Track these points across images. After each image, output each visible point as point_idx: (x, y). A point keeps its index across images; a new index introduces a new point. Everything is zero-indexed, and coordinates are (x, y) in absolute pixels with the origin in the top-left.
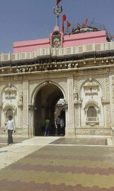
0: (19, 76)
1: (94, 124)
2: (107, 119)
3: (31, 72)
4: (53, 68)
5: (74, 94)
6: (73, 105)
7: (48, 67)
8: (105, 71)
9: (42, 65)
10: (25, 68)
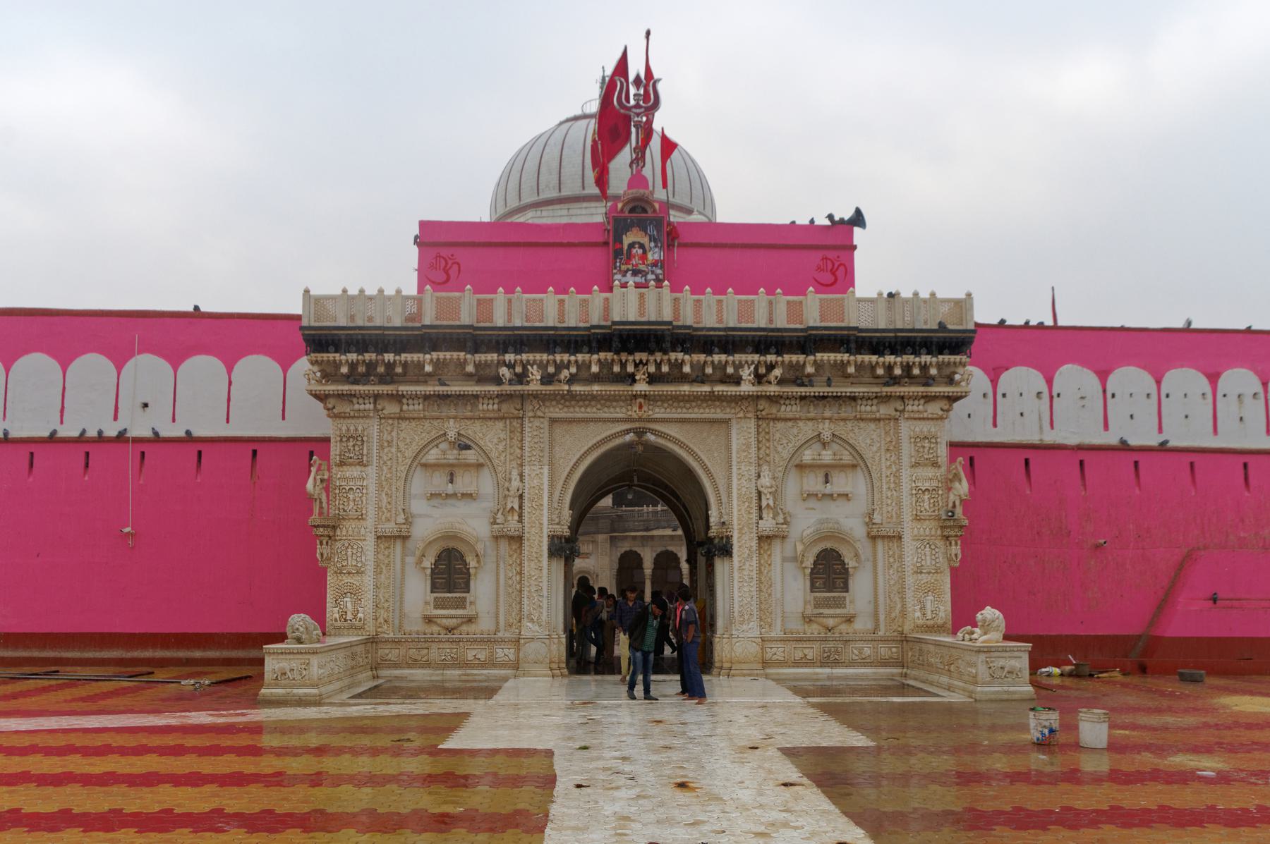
0: (504, 398)
1: (836, 620)
2: (888, 601)
3: (573, 388)
5: (759, 494)
6: (754, 543)
7: (652, 369)
8: (884, 410)
9: (624, 359)
10: (542, 366)
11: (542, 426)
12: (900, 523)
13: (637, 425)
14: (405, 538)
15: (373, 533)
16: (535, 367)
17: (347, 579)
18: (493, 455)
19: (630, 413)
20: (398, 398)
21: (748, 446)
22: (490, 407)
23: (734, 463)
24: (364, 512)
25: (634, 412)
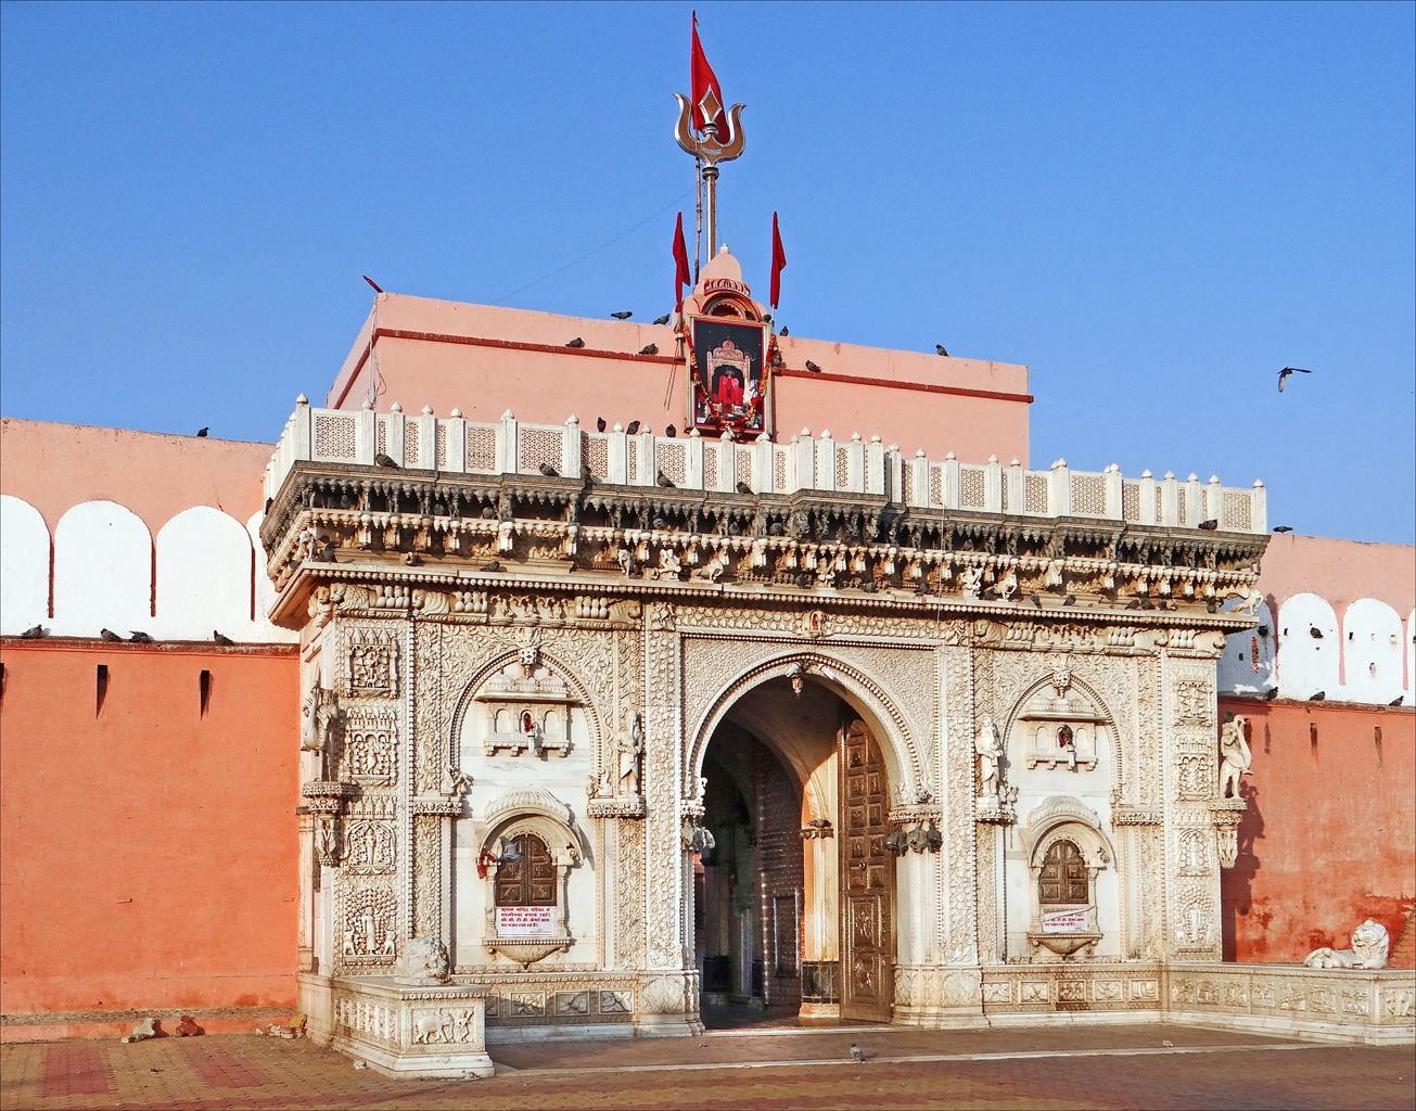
8: (1142, 640)
10: (679, 550)
11: (671, 646)
16: (670, 552)
17: (363, 884)
21: (963, 688)
23: (943, 710)
24: (393, 775)
25: (804, 625)
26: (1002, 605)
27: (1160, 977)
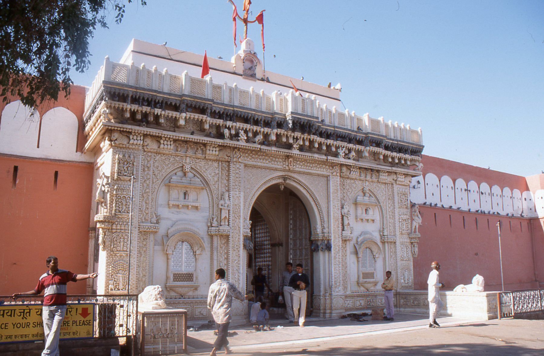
0: (222, 147)
4: (310, 148)
11: (240, 168)
12: (395, 235)
13: (286, 173)
14: (156, 232)
15: (137, 229)
16: (243, 131)
18: (211, 183)
19: (284, 166)
20: (157, 139)
21: (337, 190)
22: (214, 152)
26: (350, 162)
27: (396, 297)
